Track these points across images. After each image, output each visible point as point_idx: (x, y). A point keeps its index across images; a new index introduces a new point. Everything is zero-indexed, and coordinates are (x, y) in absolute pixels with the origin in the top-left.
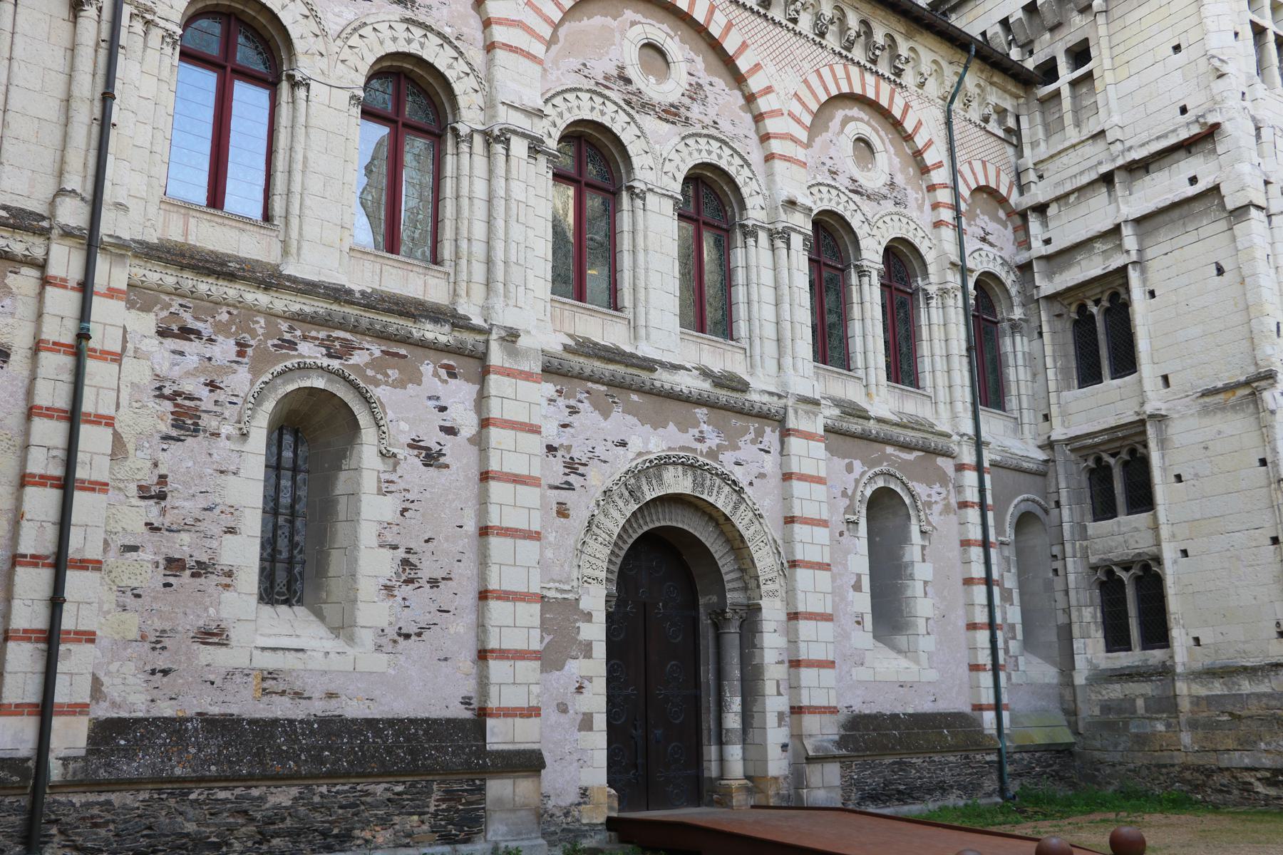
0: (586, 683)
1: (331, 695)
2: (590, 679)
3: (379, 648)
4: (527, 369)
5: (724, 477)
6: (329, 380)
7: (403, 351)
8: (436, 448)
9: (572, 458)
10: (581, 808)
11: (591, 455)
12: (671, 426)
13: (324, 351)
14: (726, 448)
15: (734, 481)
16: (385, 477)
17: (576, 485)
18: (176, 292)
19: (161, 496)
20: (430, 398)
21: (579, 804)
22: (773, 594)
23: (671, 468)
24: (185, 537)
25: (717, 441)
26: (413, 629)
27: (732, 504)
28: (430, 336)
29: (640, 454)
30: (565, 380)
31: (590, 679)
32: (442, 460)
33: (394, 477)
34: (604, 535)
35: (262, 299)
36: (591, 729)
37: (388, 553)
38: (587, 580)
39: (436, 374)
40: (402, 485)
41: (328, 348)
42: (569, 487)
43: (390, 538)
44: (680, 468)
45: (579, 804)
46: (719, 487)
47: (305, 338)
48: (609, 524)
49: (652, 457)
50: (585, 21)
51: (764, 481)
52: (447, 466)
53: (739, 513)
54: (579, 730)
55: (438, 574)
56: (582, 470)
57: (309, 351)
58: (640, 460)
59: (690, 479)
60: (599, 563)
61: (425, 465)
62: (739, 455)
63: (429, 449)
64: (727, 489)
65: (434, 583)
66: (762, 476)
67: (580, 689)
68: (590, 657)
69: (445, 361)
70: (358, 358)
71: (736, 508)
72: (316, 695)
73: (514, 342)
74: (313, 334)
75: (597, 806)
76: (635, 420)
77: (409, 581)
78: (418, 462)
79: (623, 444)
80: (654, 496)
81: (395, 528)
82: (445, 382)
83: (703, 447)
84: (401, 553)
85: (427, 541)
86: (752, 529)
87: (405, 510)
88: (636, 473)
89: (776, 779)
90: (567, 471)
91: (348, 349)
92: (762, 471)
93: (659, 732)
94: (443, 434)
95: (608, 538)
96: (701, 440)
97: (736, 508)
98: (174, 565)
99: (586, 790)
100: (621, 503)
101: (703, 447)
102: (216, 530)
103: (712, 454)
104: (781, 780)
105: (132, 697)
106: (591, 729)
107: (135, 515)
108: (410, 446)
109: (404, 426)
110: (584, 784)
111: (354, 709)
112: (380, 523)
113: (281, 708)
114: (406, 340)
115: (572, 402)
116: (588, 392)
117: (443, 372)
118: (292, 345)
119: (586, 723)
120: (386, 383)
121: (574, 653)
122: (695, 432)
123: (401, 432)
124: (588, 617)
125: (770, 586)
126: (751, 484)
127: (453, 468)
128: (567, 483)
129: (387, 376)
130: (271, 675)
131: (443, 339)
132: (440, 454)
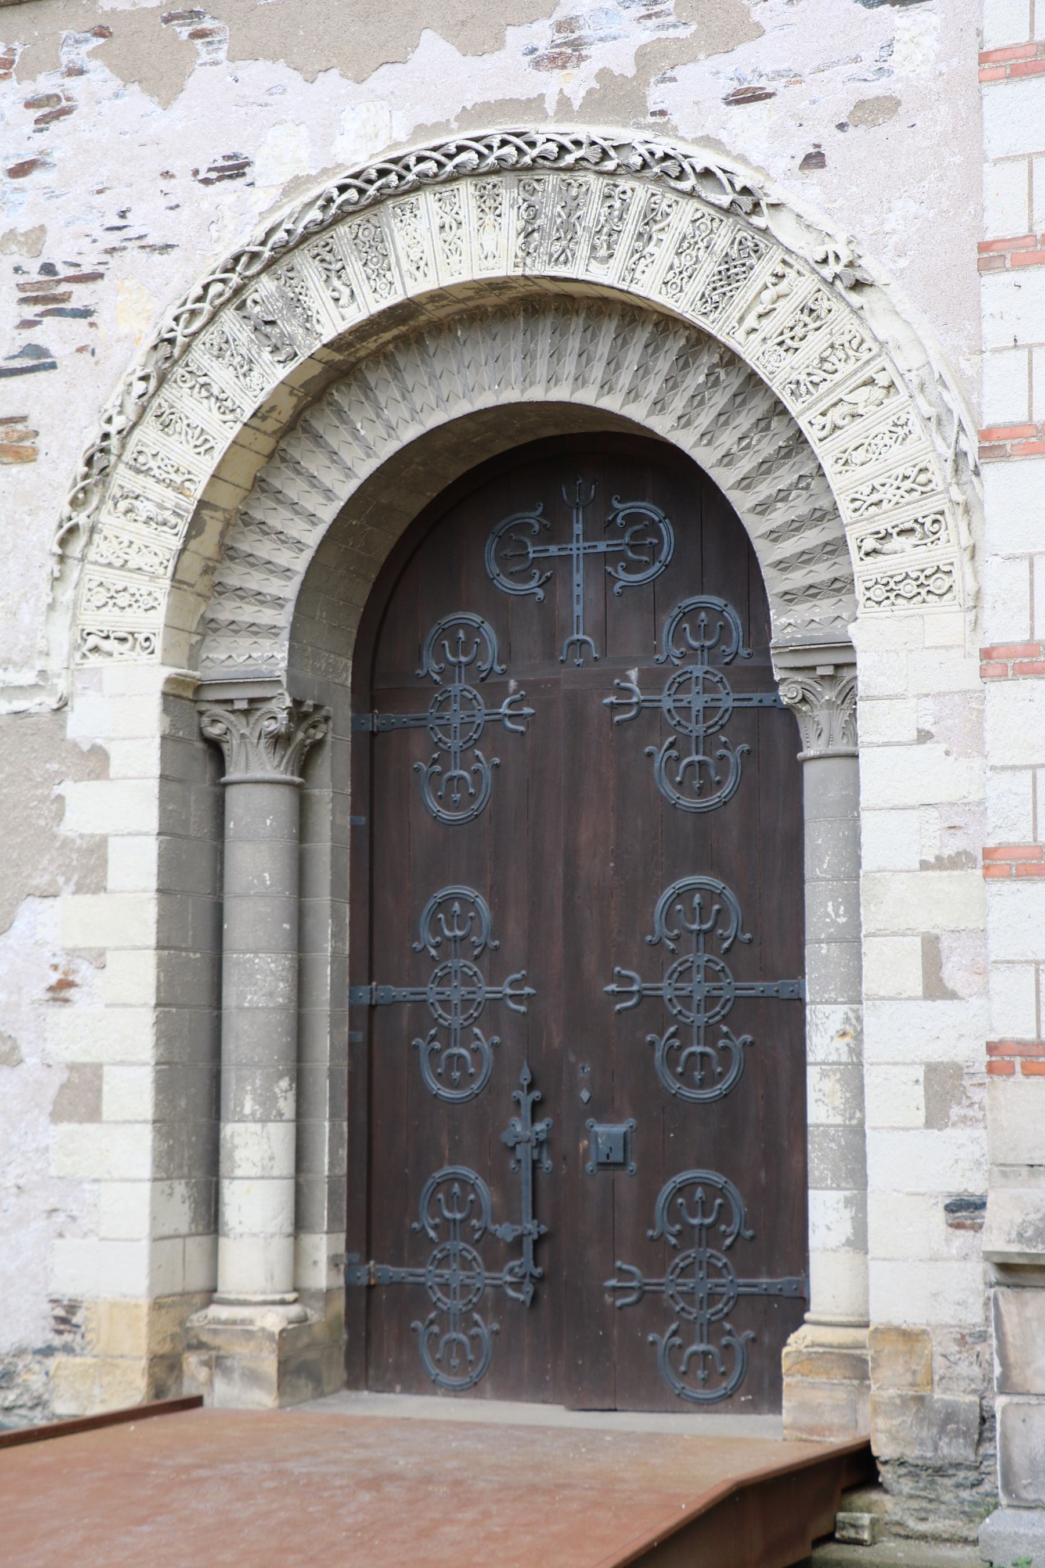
0: (84, 971)
2: (99, 959)
5: (663, 169)
9: (48, 269)
10: (52, 1363)
11: (114, 239)
12: (433, 48)
14: (686, 53)
15: (707, 174)
17: (58, 350)
21: (48, 1351)
22: (926, 585)
23: (426, 200)
25: (646, 34)
27: (709, 266)
29: (295, 185)
31: (99, 959)
36: (93, 1114)
38: (90, 645)
42: (38, 361)
44: (466, 189)
45: (48, 1351)
46: (650, 216)
49: (330, 185)
51: (891, 128)
53: (744, 295)
54: (56, 1117)
56: (80, 296)
58: (297, 203)
59: (512, 220)
60: (138, 584)
62: (747, 62)
64: (683, 215)
66: (872, 111)
67: (61, 990)
68: (100, 888)
71: (730, 274)
75: (109, 1361)
76: (279, 72)
79: (235, 169)
80: (356, 315)
83: (576, 82)
86: (815, 344)
88: (276, 255)
89: (910, 1338)
90: (30, 311)
92: (874, 89)
93: (608, 1133)
95: (170, 497)
96: (567, 52)
97: (730, 274)
99: (72, 1308)
100: (221, 376)
101: (576, 82)
103: (615, 96)
104: (941, 1345)
106: (93, 1114)
110: (67, 1290)
115: (46, 84)
116: (101, 32)
119: (80, 1096)
121: (40, 881)
122: (542, 34)
124: (95, 762)
125: (906, 556)
126: (815, 160)
128: (35, 351)
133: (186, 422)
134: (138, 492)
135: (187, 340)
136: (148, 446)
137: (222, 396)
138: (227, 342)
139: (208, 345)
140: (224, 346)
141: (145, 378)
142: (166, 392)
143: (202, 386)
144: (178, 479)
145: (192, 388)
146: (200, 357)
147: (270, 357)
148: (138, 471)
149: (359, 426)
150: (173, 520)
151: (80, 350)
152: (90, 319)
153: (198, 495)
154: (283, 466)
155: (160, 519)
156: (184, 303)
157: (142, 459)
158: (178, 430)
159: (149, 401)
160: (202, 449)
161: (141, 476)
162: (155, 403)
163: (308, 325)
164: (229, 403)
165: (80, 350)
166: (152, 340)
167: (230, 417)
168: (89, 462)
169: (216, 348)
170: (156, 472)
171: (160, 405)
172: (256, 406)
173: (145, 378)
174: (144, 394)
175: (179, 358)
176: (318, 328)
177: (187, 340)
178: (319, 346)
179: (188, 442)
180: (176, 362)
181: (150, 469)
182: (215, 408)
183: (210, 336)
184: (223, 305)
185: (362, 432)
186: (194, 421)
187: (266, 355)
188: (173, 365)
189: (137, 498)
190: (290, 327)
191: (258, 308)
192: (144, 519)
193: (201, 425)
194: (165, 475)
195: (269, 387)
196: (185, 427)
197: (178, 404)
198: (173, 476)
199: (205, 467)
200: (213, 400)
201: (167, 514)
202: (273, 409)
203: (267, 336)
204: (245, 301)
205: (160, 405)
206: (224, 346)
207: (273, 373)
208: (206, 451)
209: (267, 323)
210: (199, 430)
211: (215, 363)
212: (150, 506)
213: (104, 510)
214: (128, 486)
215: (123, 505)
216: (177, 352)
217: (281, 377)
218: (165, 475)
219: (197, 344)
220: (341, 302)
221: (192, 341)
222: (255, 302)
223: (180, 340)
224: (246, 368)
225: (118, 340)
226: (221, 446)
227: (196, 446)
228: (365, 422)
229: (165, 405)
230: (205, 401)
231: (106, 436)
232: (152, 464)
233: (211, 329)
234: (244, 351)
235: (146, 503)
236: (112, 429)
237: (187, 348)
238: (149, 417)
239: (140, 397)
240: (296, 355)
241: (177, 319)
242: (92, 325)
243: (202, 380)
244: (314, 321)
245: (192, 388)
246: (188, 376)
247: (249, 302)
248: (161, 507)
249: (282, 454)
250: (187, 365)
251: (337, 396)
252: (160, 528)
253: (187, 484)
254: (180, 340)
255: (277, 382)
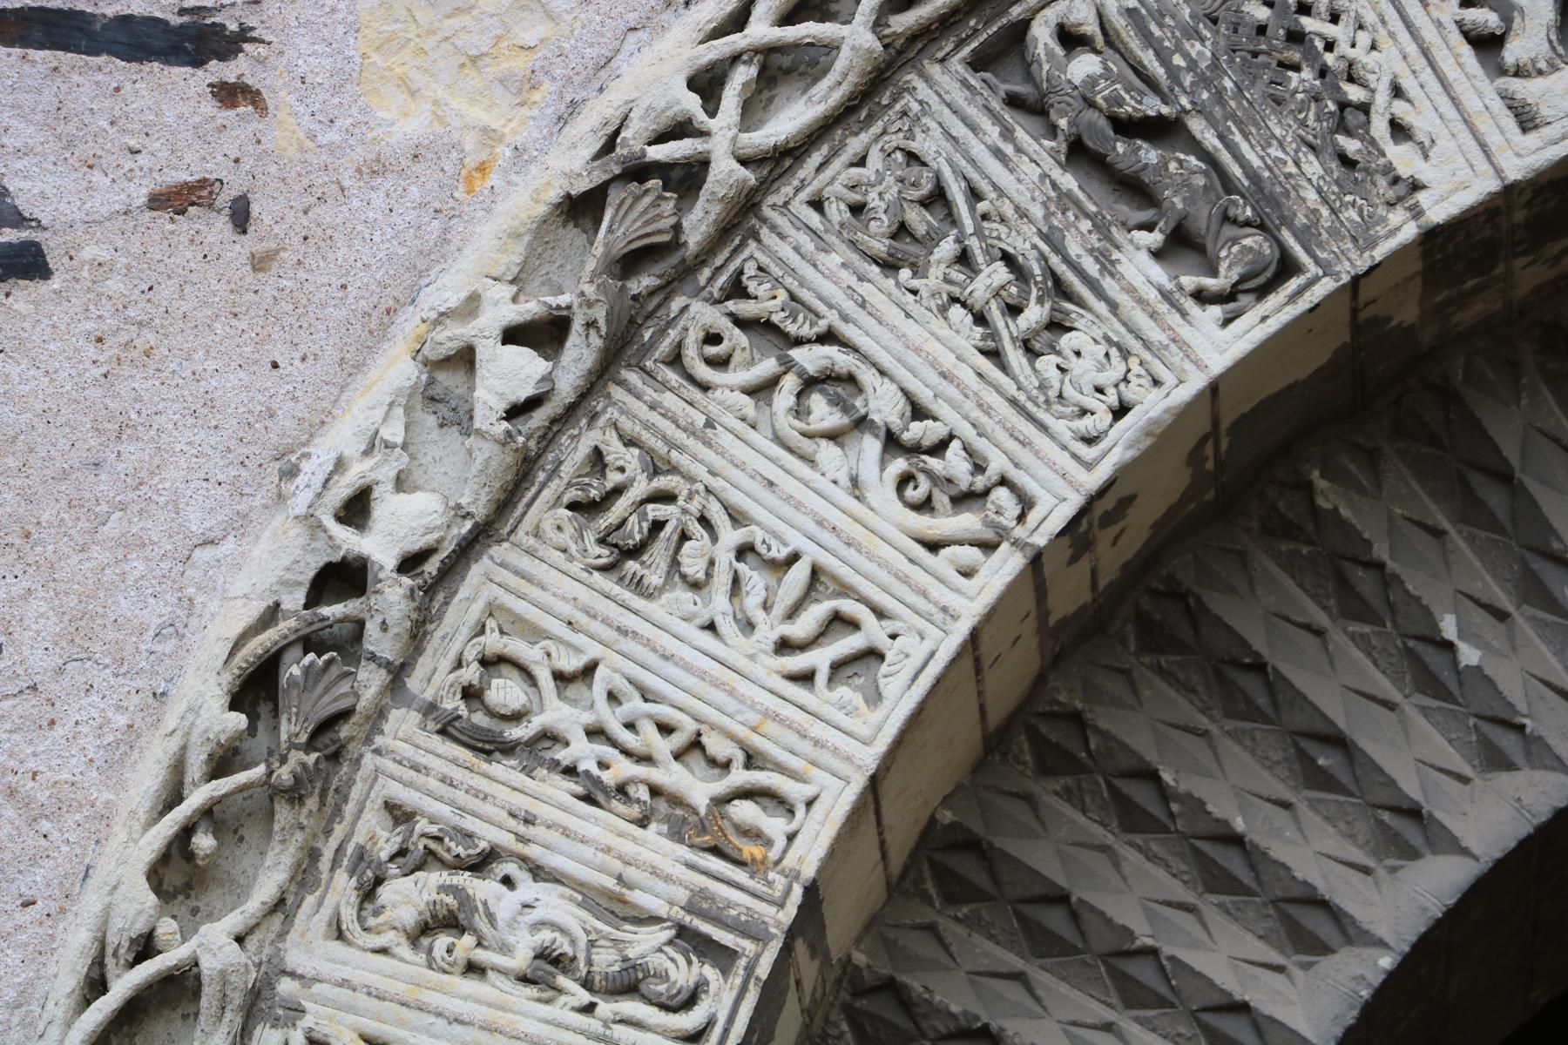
34: (594, 841)
48: (698, 659)
95: (663, 868)
100: (914, 342)
133: (730, 537)
134: (489, 835)
135: (749, 176)
136: (535, 634)
137: (915, 431)
138: (937, 198)
139: (837, 212)
140: (918, 219)
141: (543, 334)
142: (638, 404)
143: (810, 383)
144: (699, 789)
145: (762, 390)
146: (799, 257)
147: (1158, 273)
148: (489, 746)
149: (1449, 627)
150: (682, 972)
151: (175, 200)
152: (218, 70)
153: (808, 856)
154: (1048, 792)
155: (606, 961)
156: (738, 20)
157: (505, 691)
158: (693, 566)
159: (548, 437)
160: (820, 658)
161: (504, 769)
162: (574, 452)
163: (1351, 146)
164: (955, 463)
165: (175, 200)
166: (570, 165)
167: (969, 522)
168: (256, 688)
169: (881, 224)
170: (582, 752)
171: (597, 459)
172: (1093, 480)
173: (543, 334)
174: (533, 403)
175: (702, 259)
176: (1403, 158)
177: (749, 176)
178: (1409, 232)
179: (749, 626)
180: (686, 271)
181: (549, 737)
182: (881, 491)
183: (865, 168)
184: (926, 36)
185: (1469, 655)
186: (777, 529)
187: (1139, 264)
188: (667, 289)
189: (481, 864)
190: (1274, 148)
191: (1084, 66)
192: (521, 959)
193: (811, 553)
194: (623, 769)
195: (1152, 406)
196: (725, 557)
197: (694, 459)
198: (673, 776)
199: (837, 745)
200: (871, 446)
201: (646, 943)
202: (1126, 502)
203: (1135, 188)
204: (1020, 30)
205: (597, 459)
206: (918, 219)
207: (1176, 348)
208: (837, 667)
209: (1129, 127)
210: (800, 572)
211: (879, 289)
212: (553, 903)
213: (311, 919)
214: (434, 809)
215: (408, 896)
216: (698, 223)
217: (1218, 363)
218: (623, 769)
219: (788, 203)
220: (1513, 52)
221: (765, 186)
222: (1070, 39)
223: (725, 174)
224: (1034, 314)
225: (376, 169)
226: (919, 653)
227: (785, 646)
228: (1478, 617)
229: (615, 451)
230: (827, 452)
231: (342, 578)
232: (557, 713)
233: (855, 145)
234: (1023, 243)
235: (528, 888)
236: (379, 545)
237: (743, 214)
238: (544, 512)
239: (516, 412)
240: (1287, 267)
241: (707, 84)
242: (229, 94)
243: (810, 358)
244: (1379, 128)
245: (762, 390)
246: (736, 338)
247: (1042, 34)
248: (615, 907)
249: (1054, 733)
250: (737, 289)
251: (1327, 494)
252: (605, 1008)
253: (744, 811)
254: (725, 174)
255: (1196, 382)
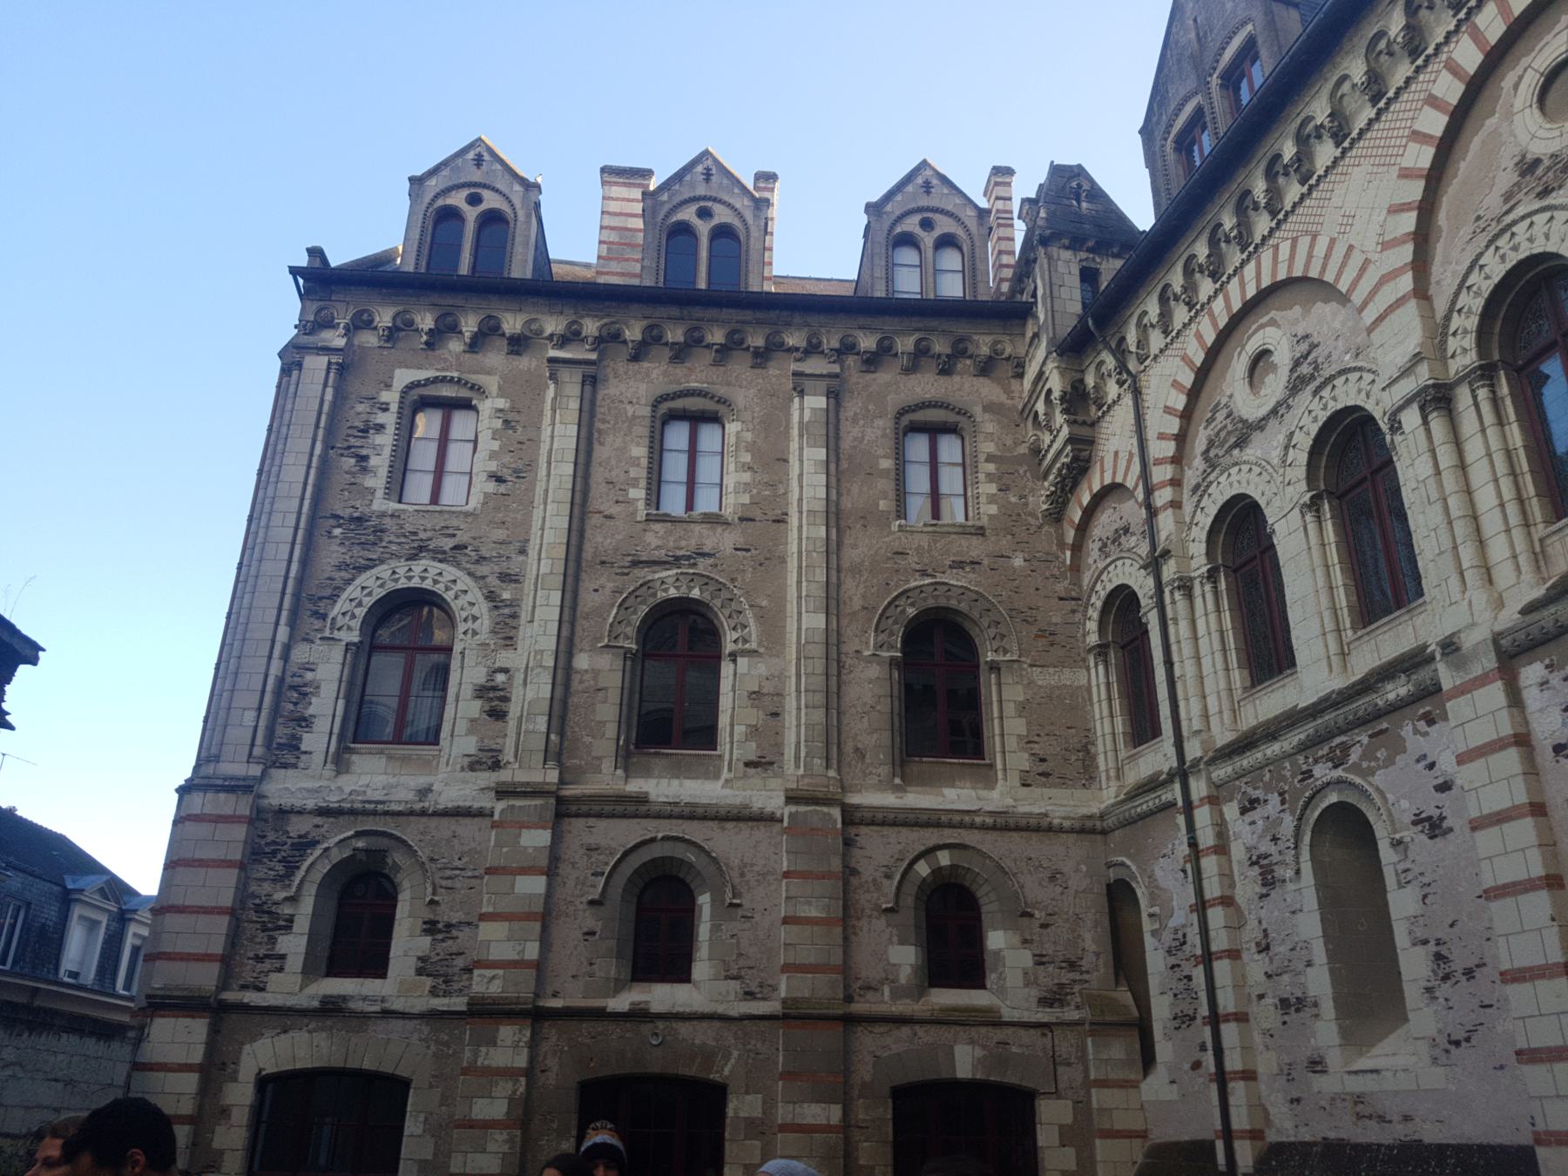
1: (1407, 1118)
3: (1435, 1060)
4: (1480, 672)
6: (1340, 791)
7: (1385, 725)
8: (1435, 813)
13: (1330, 764)
16: (1401, 867)
18: (1239, 776)
19: (1267, 948)
20: (1418, 761)
24: (1286, 977)
26: (1459, 1035)
28: (1391, 696)
30: (1552, 646)
32: (1445, 825)
33: (1408, 865)
35: (1274, 749)
37: (1420, 949)
39: (1416, 731)
40: (1416, 869)
41: (1332, 760)
43: (1420, 934)
47: (1316, 761)
50: (1463, 165)
52: (1451, 830)
55: (1471, 962)
57: (1323, 772)
61: (1431, 838)
63: (1430, 818)
65: (1469, 973)
69: (1421, 711)
70: (1354, 756)
72: (1396, 1118)
73: (1458, 649)
74: (1320, 753)
77: (1446, 978)
78: (1423, 837)
81: (1421, 920)
82: (1426, 734)
84: (1432, 947)
85: (1452, 926)
87: (1425, 897)
91: (1346, 749)
94: (1439, 795)
98: (1284, 1004)
102: (1301, 966)
105: (1285, 1127)
107: (1256, 967)
108: (1415, 823)
109: (1405, 804)
111: (1431, 1134)
112: (1408, 918)
113: (1370, 1134)
114: (1379, 714)
117: (1422, 725)
118: (1308, 774)
120: (1379, 768)
123: (1405, 809)
127: (1457, 828)
129: (1377, 759)
130: (1359, 1099)
131: (1403, 691)
132: (1442, 818)
